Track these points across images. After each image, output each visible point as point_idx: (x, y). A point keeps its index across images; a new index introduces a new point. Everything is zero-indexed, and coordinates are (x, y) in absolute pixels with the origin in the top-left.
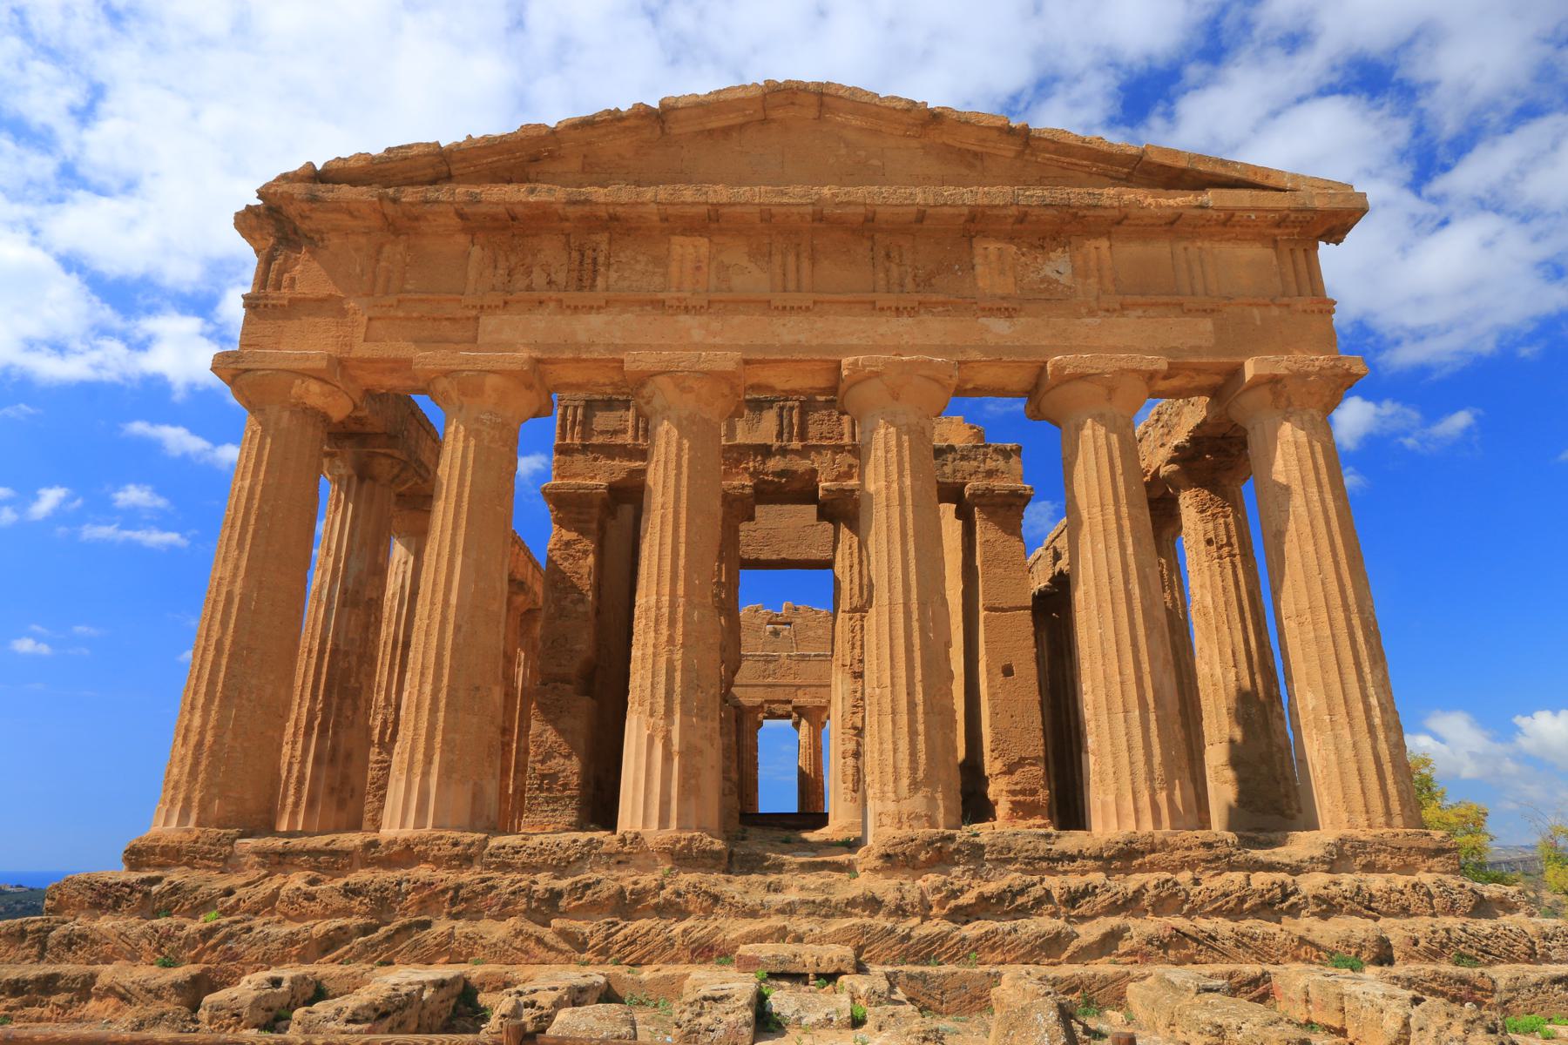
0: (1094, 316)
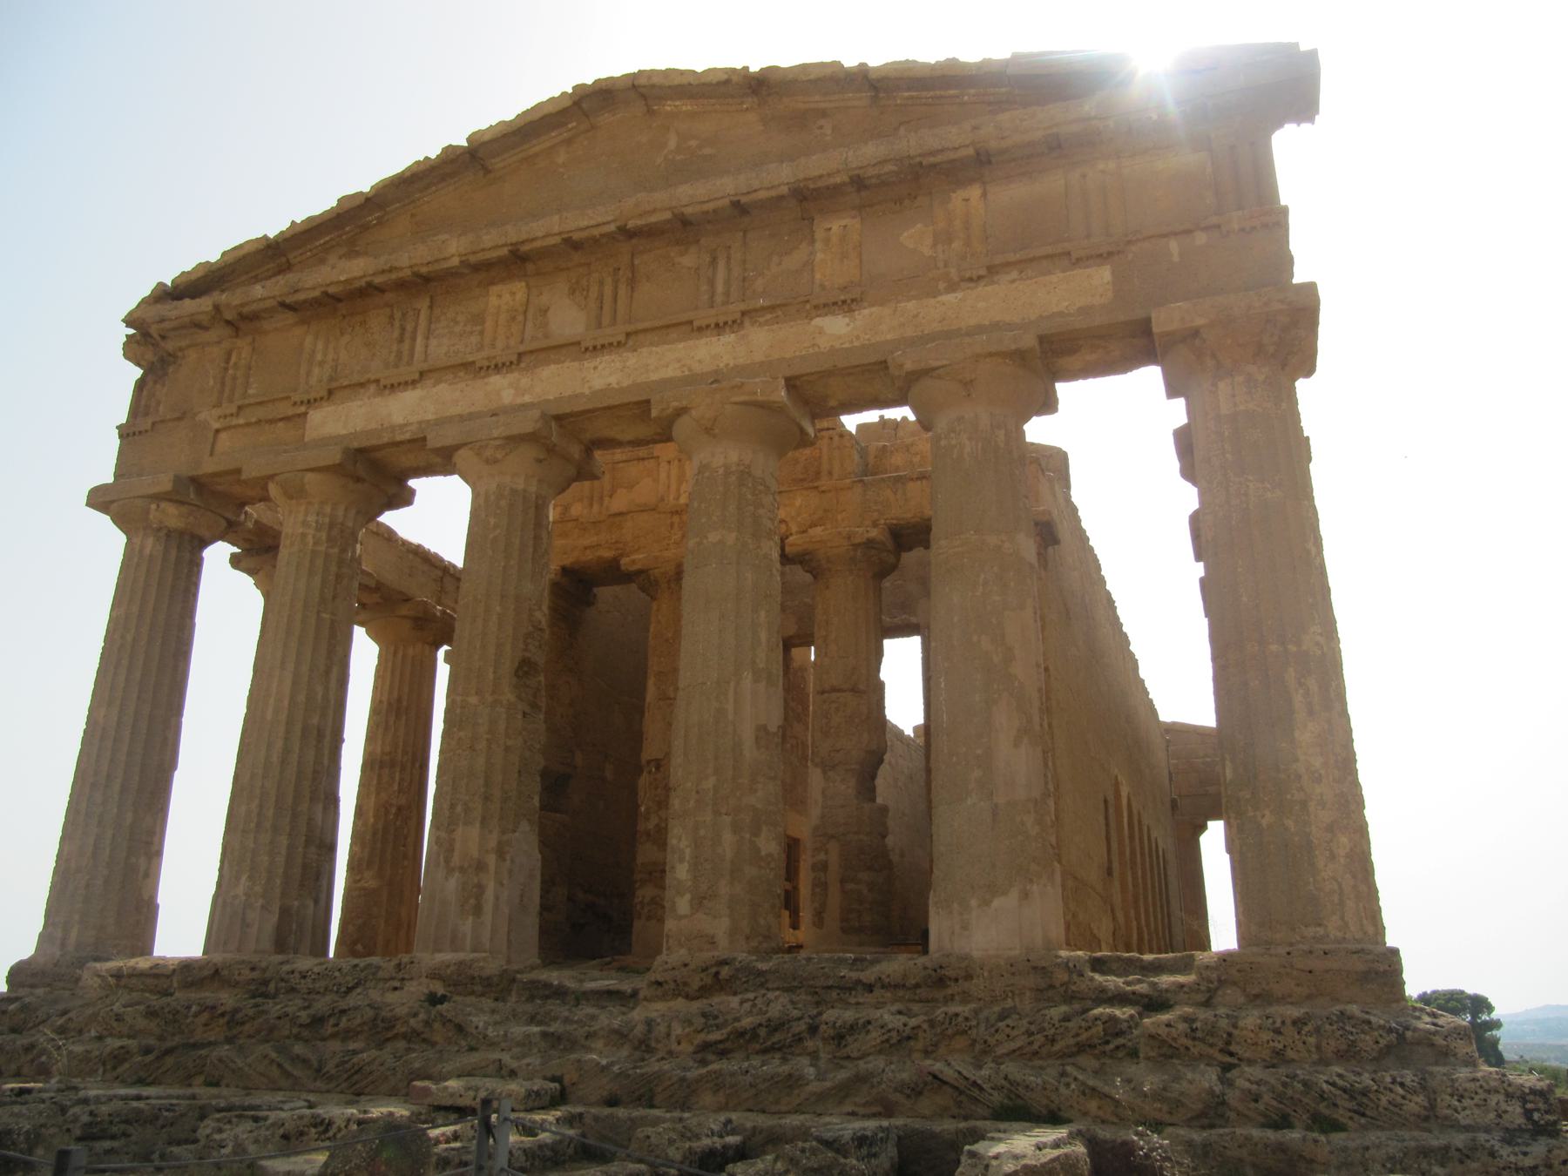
0: (954, 291)
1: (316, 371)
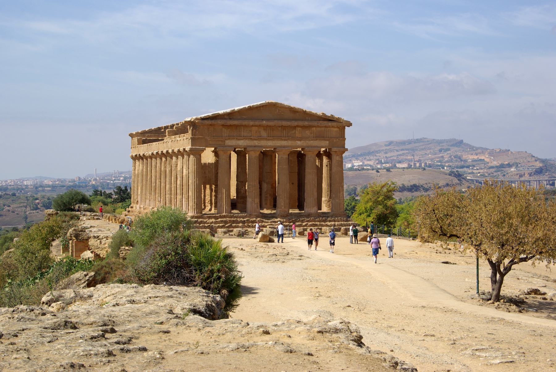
1: (226, 134)
